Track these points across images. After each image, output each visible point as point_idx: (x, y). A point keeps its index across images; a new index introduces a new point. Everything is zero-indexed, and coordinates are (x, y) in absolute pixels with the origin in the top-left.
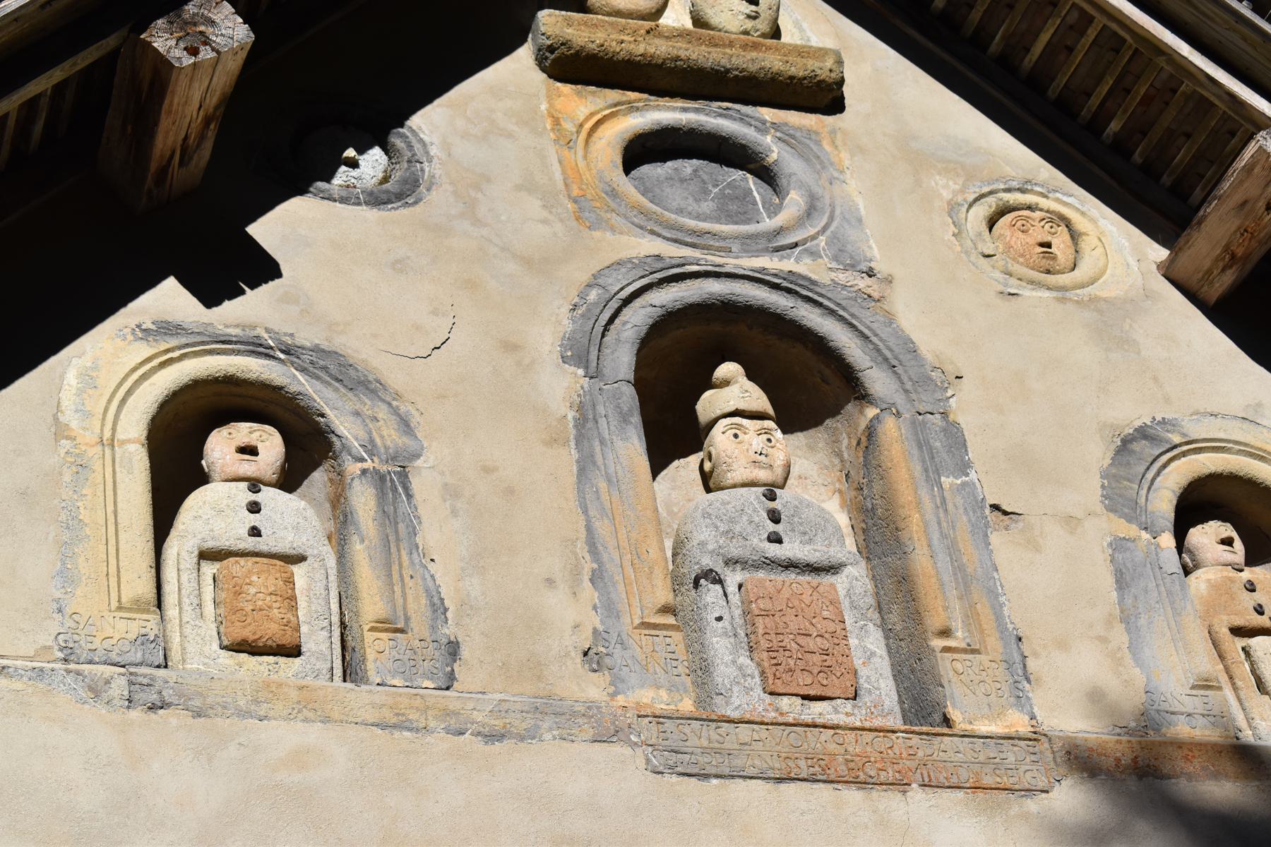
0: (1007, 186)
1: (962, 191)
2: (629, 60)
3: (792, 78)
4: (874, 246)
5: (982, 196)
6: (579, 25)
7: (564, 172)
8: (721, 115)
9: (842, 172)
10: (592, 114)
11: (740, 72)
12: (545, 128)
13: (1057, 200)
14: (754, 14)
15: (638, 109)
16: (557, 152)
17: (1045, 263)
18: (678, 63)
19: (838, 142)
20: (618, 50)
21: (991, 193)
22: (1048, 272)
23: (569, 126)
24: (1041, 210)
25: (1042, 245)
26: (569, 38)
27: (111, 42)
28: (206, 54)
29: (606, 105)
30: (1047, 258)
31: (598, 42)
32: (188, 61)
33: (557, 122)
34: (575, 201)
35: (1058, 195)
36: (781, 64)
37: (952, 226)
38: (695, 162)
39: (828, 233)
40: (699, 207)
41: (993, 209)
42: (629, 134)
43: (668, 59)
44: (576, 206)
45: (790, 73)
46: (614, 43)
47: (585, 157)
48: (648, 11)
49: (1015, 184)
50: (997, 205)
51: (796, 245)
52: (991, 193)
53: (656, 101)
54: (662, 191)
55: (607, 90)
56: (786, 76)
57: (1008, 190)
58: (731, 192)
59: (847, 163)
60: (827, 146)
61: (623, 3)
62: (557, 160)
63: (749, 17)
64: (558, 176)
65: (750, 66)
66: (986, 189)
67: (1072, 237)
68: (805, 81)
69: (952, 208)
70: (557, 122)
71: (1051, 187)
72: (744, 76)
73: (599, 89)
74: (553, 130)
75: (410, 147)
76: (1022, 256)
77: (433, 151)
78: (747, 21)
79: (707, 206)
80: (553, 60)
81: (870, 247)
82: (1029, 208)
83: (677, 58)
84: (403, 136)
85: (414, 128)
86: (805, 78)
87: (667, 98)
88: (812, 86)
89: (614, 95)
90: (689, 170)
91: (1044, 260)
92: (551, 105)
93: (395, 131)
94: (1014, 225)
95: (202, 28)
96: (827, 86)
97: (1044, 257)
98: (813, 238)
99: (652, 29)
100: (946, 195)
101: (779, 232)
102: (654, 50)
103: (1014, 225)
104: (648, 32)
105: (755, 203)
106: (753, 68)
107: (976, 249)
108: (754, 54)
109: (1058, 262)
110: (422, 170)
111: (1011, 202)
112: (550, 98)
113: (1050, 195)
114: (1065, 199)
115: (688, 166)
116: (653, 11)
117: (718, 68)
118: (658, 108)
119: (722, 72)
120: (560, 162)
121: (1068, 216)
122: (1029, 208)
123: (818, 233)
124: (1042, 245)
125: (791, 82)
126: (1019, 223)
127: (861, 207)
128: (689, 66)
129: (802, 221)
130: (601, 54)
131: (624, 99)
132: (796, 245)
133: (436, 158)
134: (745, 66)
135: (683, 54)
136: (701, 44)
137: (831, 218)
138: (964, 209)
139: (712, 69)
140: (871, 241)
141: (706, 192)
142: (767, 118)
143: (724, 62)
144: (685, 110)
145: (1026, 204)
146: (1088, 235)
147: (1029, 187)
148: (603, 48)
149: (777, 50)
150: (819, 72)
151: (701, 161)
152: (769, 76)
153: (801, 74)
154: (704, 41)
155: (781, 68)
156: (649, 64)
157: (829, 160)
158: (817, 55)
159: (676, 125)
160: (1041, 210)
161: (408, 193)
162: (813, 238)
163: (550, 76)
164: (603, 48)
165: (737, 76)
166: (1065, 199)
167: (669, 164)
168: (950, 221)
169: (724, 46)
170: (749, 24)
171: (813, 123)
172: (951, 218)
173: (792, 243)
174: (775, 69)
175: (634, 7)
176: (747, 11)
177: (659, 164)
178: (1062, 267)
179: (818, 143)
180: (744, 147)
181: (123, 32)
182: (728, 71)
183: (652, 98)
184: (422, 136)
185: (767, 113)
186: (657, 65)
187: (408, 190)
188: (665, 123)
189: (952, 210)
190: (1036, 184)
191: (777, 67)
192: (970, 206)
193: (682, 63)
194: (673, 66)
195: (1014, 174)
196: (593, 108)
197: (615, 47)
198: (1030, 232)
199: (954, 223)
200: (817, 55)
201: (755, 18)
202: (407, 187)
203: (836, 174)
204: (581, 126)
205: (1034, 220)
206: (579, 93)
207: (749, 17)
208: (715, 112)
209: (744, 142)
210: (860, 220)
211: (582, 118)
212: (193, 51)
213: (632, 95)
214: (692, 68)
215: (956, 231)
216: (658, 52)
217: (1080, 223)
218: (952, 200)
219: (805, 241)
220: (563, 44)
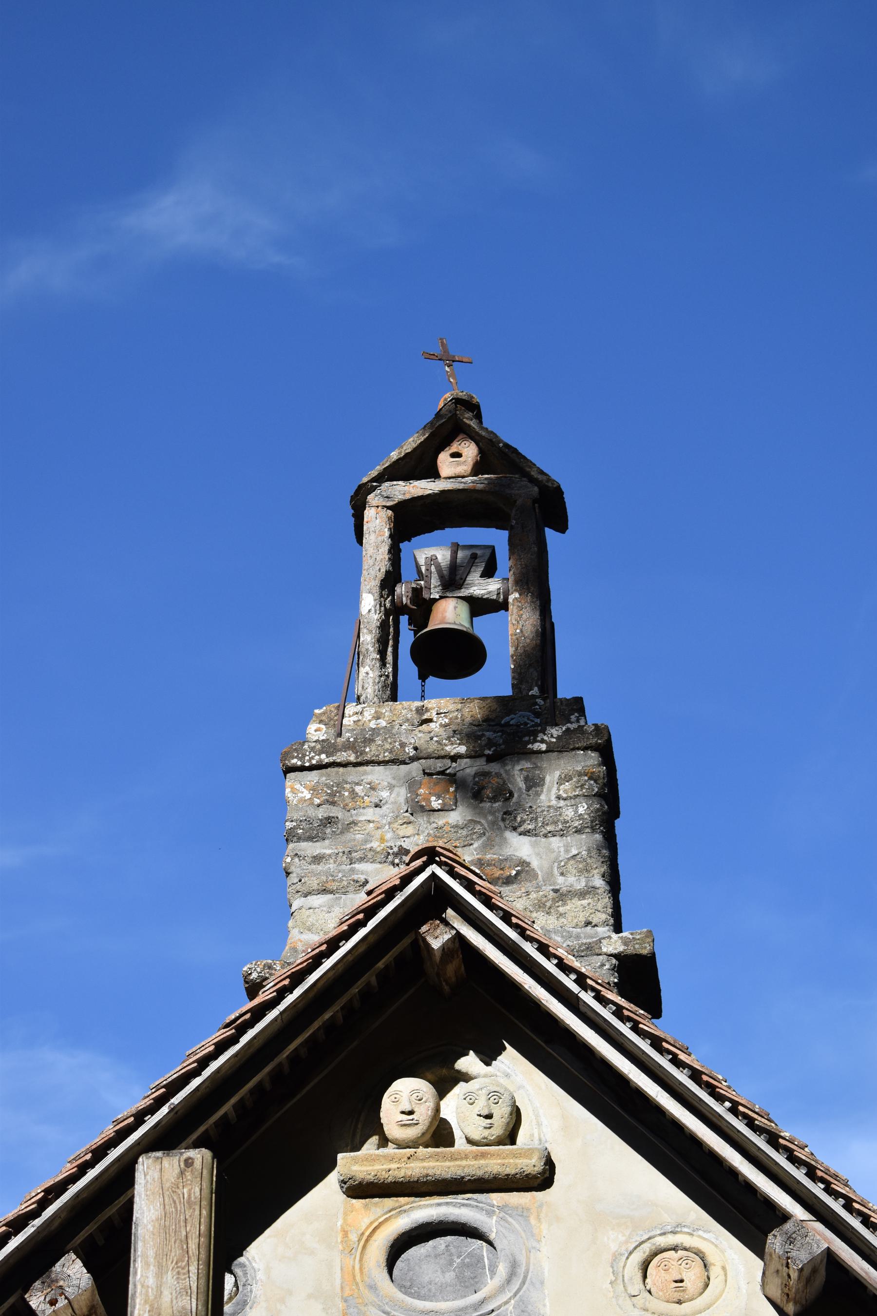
0: (662, 1231)
1: (626, 1242)
2: (395, 1181)
3: (508, 1175)
4: (548, 1304)
5: (643, 1242)
6: (362, 1161)
7: (342, 1277)
8: (463, 1205)
9: (539, 1241)
10: (372, 1223)
11: (472, 1177)
12: (337, 1242)
13: (699, 1236)
14: (489, 1126)
15: (405, 1211)
16: (341, 1261)
17: (677, 1296)
18: (428, 1178)
19: (542, 1215)
20: (387, 1177)
21: (649, 1239)
22: (679, 1302)
23: (353, 1237)
24: (685, 1249)
25: (676, 1282)
26: (353, 1174)
27: (11, 1300)
28: (62, 1303)
29: (382, 1213)
30: (678, 1291)
31: (373, 1174)
32: (50, 1310)
33: (345, 1234)
34: (346, 1301)
35: (701, 1233)
36: (499, 1167)
37: (612, 1274)
38: (449, 1238)
39: (518, 1296)
40: (444, 1277)
41: (647, 1254)
42: (394, 1236)
43: (421, 1177)
44: (345, 1304)
45: (506, 1173)
46: (384, 1172)
47: (361, 1260)
48: (415, 1137)
49: (669, 1228)
50: (651, 1250)
51: (493, 1311)
52: (649, 1239)
53: (419, 1201)
54: (421, 1268)
55: (386, 1199)
56: (504, 1175)
57: (664, 1234)
58: (468, 1260)
59: (545, 1232)
60: (533, 1221)
61: (398, 1135)
62: (340, 1267)
63: (485, 1128)
64: (338, 1282)
65: (478, 1172)
66: (645, 1237)
67: (705, 1266)
68: (518, 1176)
69: (616, 1257)
70: (345, 1234)
71: (696, 1227)
72: (475, 1179)
73: (381, 1199)
74: (342, 1242)
75: (245, 1274)
76: (662, 1290)
77: (260, 1275)
78: (485, 1130)
79: (450, 1276)
80: (346, 1188)
81: (544, 1305)
82: (675, 1249)
83: (427, 1175)
84: (243, 1266)
85: (250, 1259)
86: (517, 1174)
87: (427, 1198)
88: (523, 1178)
89: (390, 1202)
90: (443, 1247)
91: (676, 1293)
92: (345, 1220)
93: (236, 1262)
94: (659, 1266)
95: (61, 1283)
96: (533, 1176)
97: (675, 1291)
98: (506, 1303)
99: (411, 1156)
100: (613, 1247)
101: (483, 1302)
102: (411, 1173)
103: (659, 1266)
104: (409, 1158)
105: (484, 1268)
106: (480, 1173)
107: (626, 1290)
108: (482, 1162)
109: (687, 1292)
110: (251, 1291)
111: (662, 1245)
112: (345, 1214)
113: (695, 1233)
114: (705, 1235)
115: (441, 1243)
116: (419, 1135)
117: (456, 1177)
118: (420, 1207)
119: (459, 1179)
120: (342, 1269)
121: (703, 1250)
122: (675, 1249)
123: (510, 1299)
124: (676, 1282)
125: (508, 1177)
126: (662, 1265)
127: (546, 1271)
128: (436, 1179)
129: (501, 1289)
130: (376, 1181)
131: (397, 1205)
132: (493, 1311)
133: (260, 1281)
134: (474, 1173)
135: (430, 1172)
136: (446, 1160)
137: (523, 1283)
138: (624, 1258)
139: (452, 1178)
140: (547, 1300)
141: (451, 1263)
142: (495, 1203)
143: (460, 1173)
144: (439, 1205)
145: (674, 1245)
146: (715, 1265)
147: (679, 1230)
148: (377, 1177)
149: (498, 1155)
150: (525, 1169)
151: (453, 1237)
152: (492, 1176)
153: (513, 1172)
154: (447, 1158)
155: (499, 1170)
156: (409, 1182)
157: (532, 1232)
158: (526, 1154)
159: (429, 1220)
160: (685, 1249)
161: (239, 1311)
162: (506, 1303)
163: (348, 1196)
164: (377, 1177)
165: (470, 1180)
166: (705, 1235)
167: (431, 1243)
168: (611, 1270)
169: (462, 1159)
170: (486, 1133)
171: (527, 1201)
172: (613, 1267)
173: (489, 1311)
174: (495, 1172)
175: (405, 1136)
176: (484, 1125)
177: (423, 1244)
178: (690, 1296)
179: (527, 1219)
180: (476, 1228)
181: (19, 1292)
182: (463, 1178)
183: (418, 1199)
184: (254, 1264)
185: (496, 1198)
186: (414, 1182)
187: (239, 1309)
188: (421, 1221)
189: (614, 1260)
190: (684, 1226)
191: (496, 1170)
192: (631, 1253)
193: (431, 1178)
194: (425, 1180)
195: (669, 1220)
196: (372, 1218)
197: (384, 1175)
198: (670, 1270)
199: (613, 1272)
200: (526, 1154)
201: (490, 1128)
202: (239, 1307)
203: (535, 1244)
204: (363, 1234)
205: (673, 1260)
206: (366, 1206)
207: (485, 1128)
208: (459, 1203)
209: (475, 1226)
210: (542, 1283)
211: (364, 1228)
212: (53, 1302)
213: (403, 1200)
214: (438, 1180)
215: (614, 1279)
216: (414, 1174)
217: (712, 1256)
218: (617, 1251)
219: (499, 1307)
220: (350, 1179)
